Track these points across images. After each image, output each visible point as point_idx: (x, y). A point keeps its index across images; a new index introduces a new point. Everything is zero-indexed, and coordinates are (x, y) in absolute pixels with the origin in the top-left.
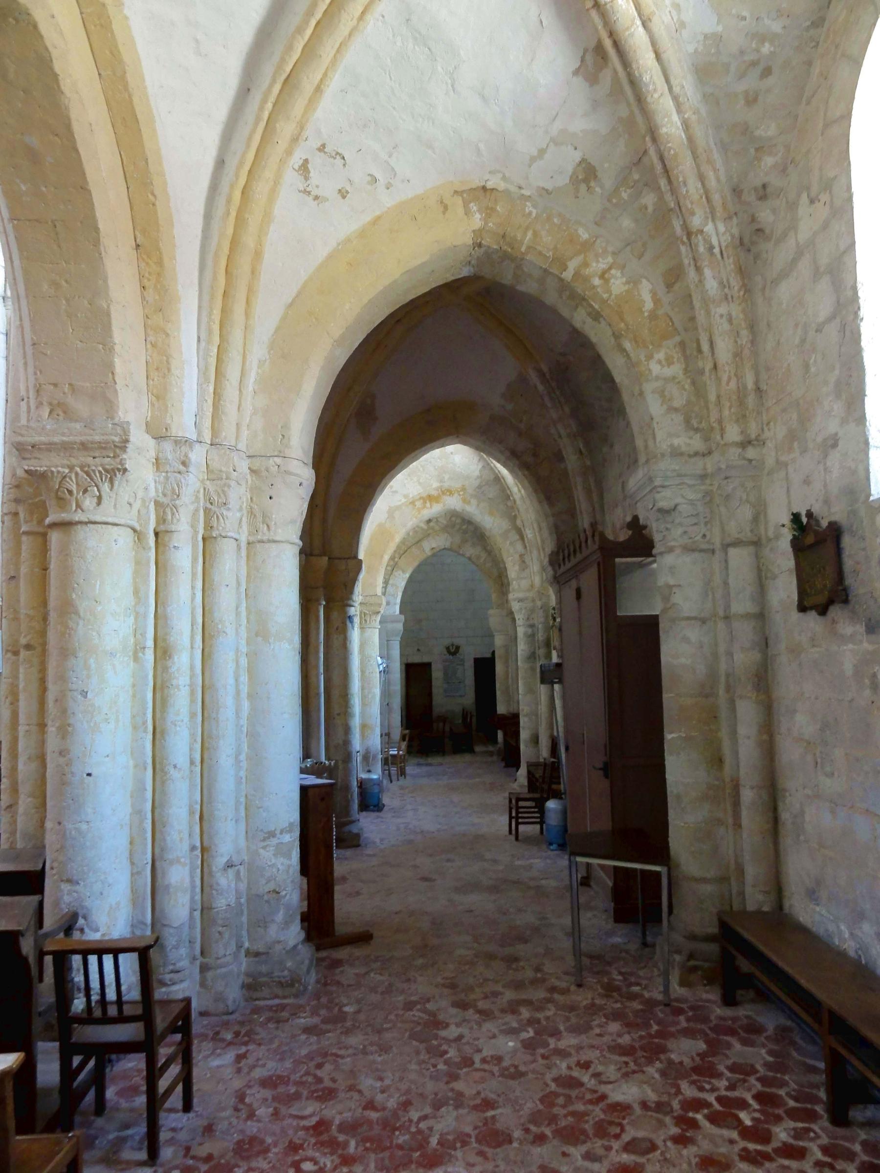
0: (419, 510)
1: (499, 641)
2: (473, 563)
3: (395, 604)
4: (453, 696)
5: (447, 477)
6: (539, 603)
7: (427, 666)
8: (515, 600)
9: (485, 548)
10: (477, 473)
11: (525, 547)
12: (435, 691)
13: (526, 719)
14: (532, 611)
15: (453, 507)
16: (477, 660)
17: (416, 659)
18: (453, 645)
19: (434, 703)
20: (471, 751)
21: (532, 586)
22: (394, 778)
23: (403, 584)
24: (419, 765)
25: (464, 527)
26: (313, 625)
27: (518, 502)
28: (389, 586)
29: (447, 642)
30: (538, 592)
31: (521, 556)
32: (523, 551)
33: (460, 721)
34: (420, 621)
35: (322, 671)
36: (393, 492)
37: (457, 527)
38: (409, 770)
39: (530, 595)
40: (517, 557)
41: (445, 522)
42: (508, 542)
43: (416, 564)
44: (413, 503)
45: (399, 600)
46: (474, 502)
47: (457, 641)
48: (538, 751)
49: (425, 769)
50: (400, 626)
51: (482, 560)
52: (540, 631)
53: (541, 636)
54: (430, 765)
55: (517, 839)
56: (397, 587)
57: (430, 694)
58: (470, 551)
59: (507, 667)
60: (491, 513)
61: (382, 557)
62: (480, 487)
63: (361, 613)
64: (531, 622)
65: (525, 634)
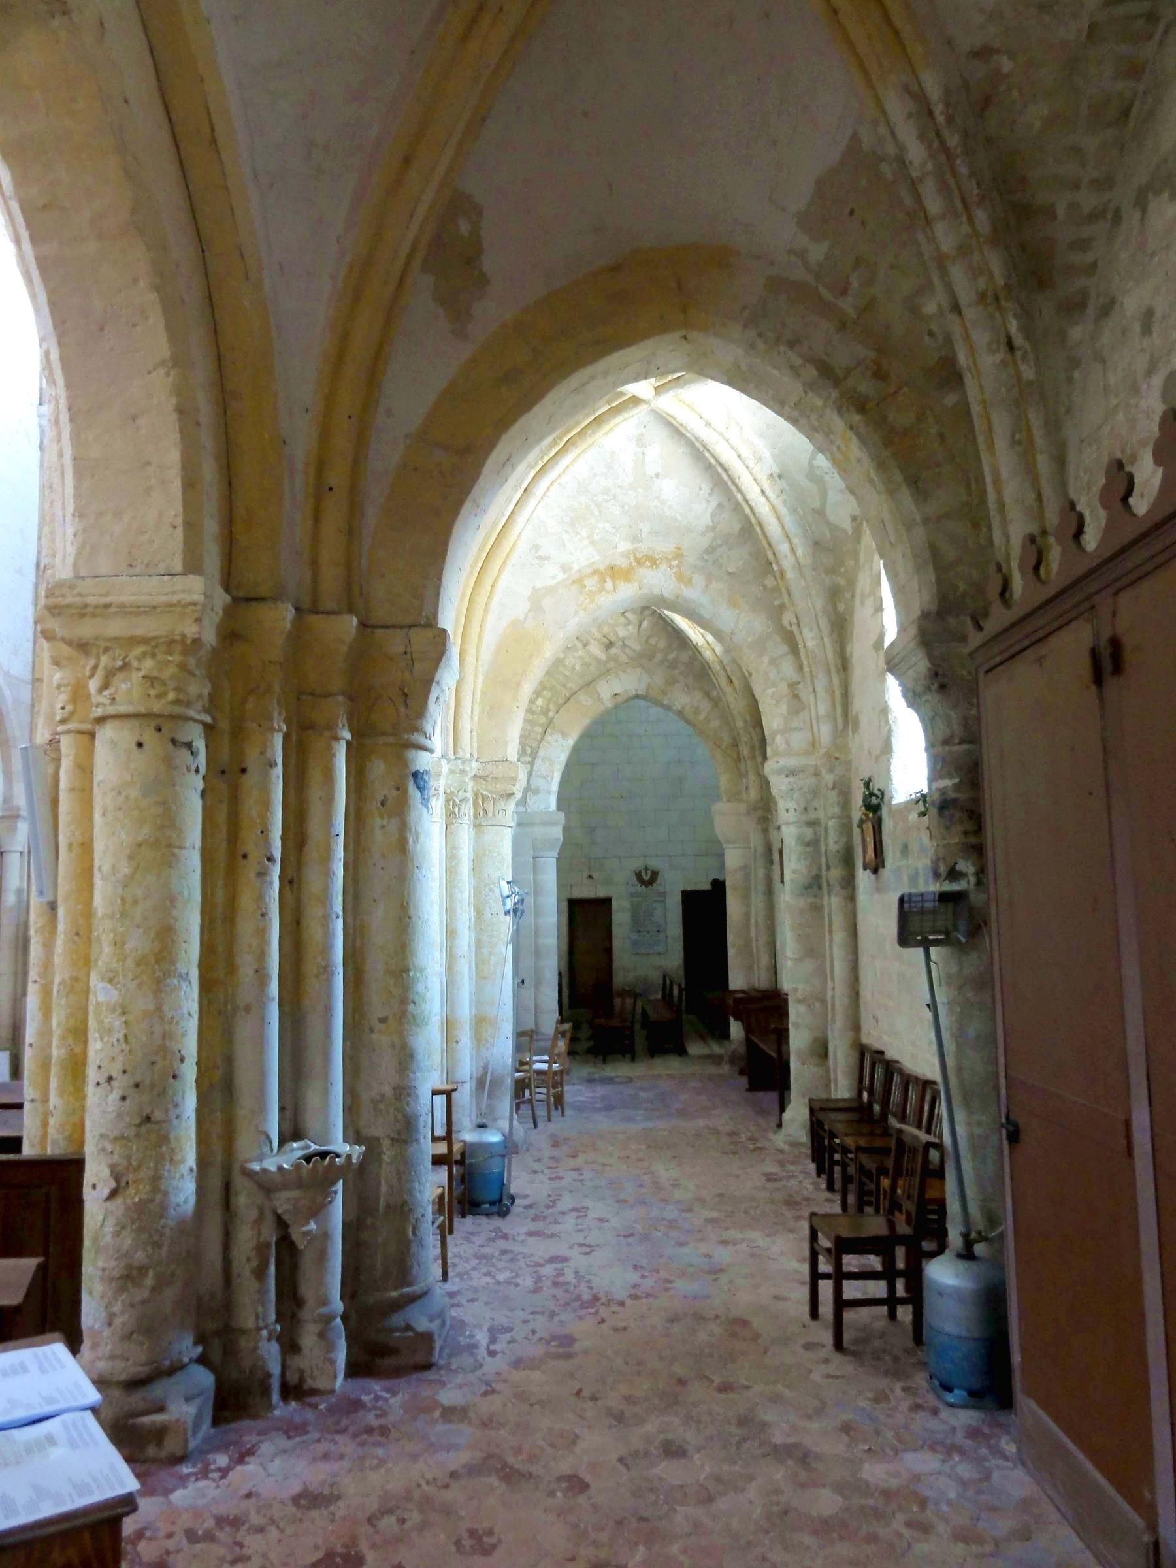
0: (591, 594)
1: (733, 859)
2: (688, 722)
3: (549, 792)
4: (649, 953)
5: (645, 528)
6: (829, 778)
7: (603, 905)
8: (779, 772)
9: (707, 695)
10: (707, 520)
11: (801, 668)
12: (616, 943)
13: (802, 1009)
14: (815, 793)
15: (656, 591)
17: (586, 892)
18: (646, 869)
19: (615, 965)
20: (681, 1052)
21: (813, 744)
22: (541, 1112)
23: (562, 757)
24: (590, 1081)
25: (671, 656)
26: (315, 793)
27: (790, 575)
28: (538, 761)
29: (638, 864)
30: (827, 754)
31: (793, 686)
32: (796, 677)
33: (659, 996)
34: (592, 830)
35: (338, 907)
36: (540, 558)
37: (659, 656)
38: (574, 1092)
39: (811, 761)
40: (783, 688)
41: (638, 648)
42: (766, 660)
43: (586, 721)
44: (579, 581)
45: (555, 786)
46: (699, 580)
47: (654, 863)
48: (827, 1071)
49: (601, 1091)
50: (557, 832)
51: (702, 717)
52: (831, 833)
53: (833, 843)
54: (610, 1081)
55: (839, 1345)
56: (552, 763)
57: (609, 951)
58: (681, 699)
59: (749, 905)
60: (733, 604)
61: (518, 685)
62: (710, 550)
63: (476, 795)
64: (812, 816)
65: (800, 839)
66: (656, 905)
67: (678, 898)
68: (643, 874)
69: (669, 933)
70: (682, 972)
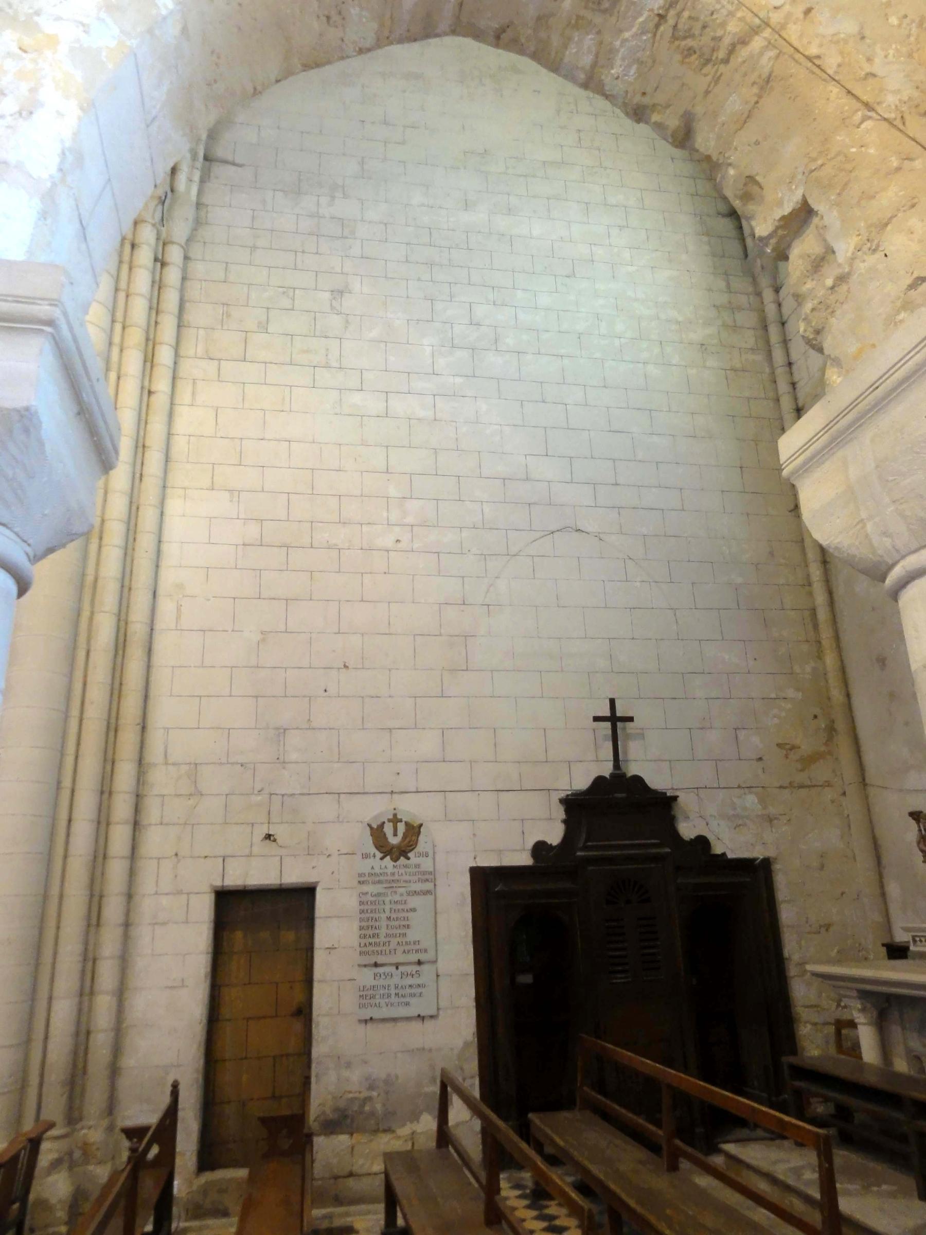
7: (294, 905)
16: (483, 879)
18: (395, 820)
19: (318, 1050)
29: (375, 809)
34: (282, 731)
47: (411, 808)
66: (414, 902)
67: (463, 886)
68: (388, 829)
69: (443, 965)
70: (473, 1066)
